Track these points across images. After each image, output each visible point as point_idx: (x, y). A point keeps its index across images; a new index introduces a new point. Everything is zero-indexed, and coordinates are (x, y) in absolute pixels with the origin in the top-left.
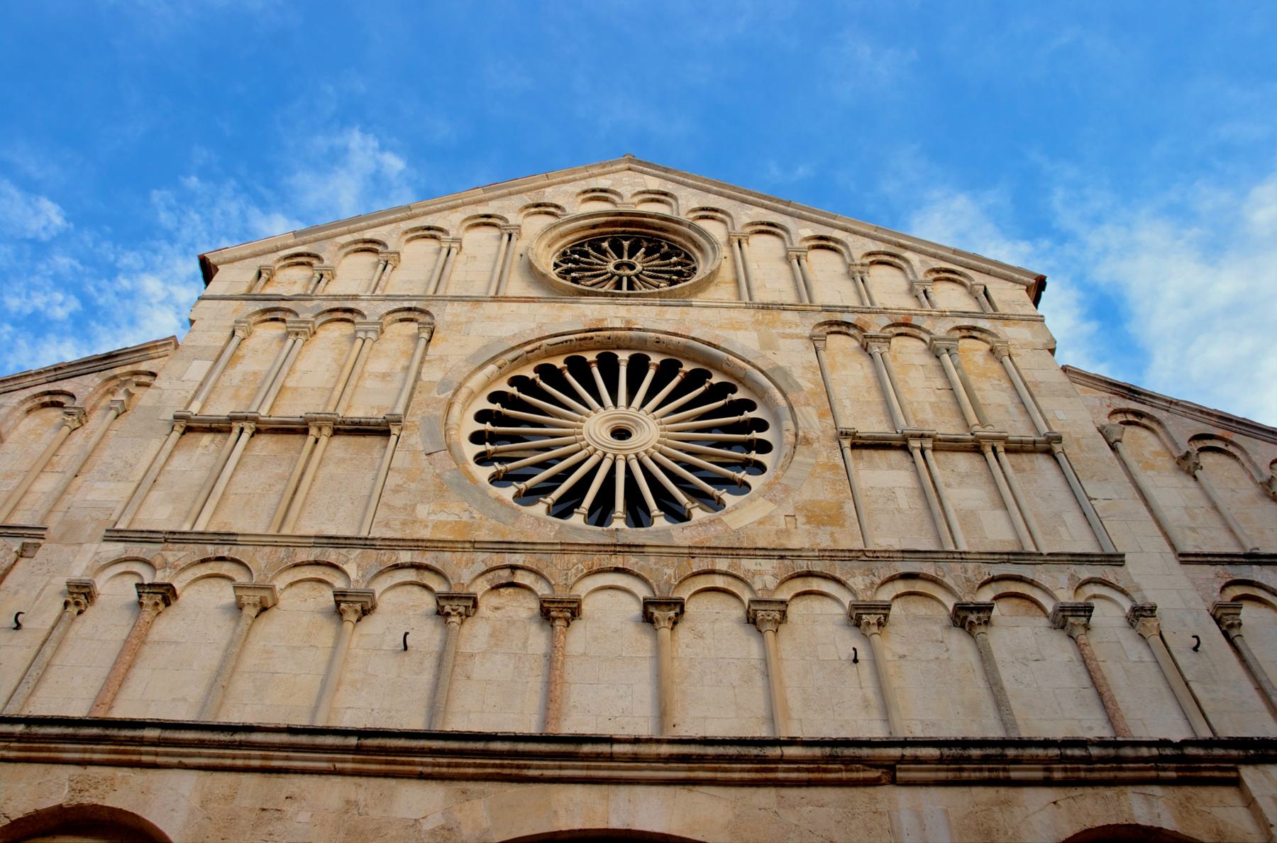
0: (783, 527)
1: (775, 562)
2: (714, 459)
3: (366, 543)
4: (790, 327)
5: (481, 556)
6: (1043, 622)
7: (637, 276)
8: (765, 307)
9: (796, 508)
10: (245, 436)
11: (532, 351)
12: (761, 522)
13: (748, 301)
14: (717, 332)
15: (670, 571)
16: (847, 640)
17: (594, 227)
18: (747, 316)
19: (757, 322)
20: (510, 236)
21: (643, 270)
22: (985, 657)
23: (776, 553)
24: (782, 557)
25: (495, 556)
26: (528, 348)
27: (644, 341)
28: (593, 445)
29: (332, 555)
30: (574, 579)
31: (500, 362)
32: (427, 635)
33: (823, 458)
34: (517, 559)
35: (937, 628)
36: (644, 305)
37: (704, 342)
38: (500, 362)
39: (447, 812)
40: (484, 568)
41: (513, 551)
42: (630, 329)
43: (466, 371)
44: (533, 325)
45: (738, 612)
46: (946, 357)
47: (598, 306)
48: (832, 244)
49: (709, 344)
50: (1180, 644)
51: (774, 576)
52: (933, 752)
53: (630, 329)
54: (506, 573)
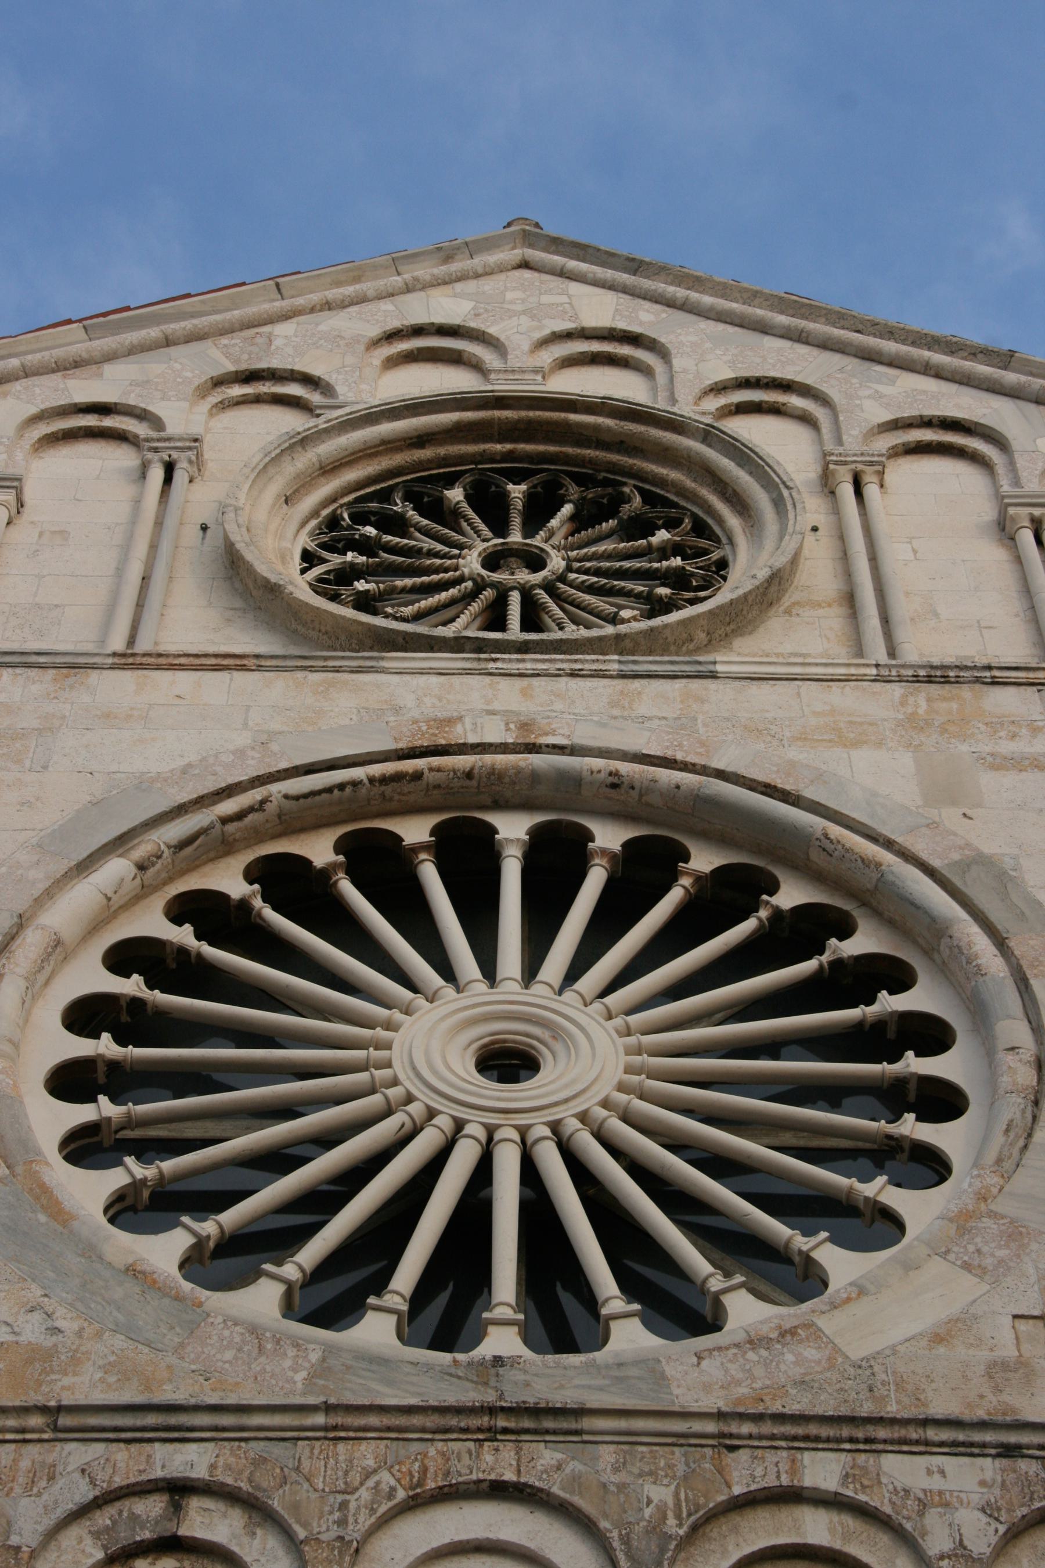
0: (1010, 1352)
1: (989, 1467)
2: (788, 1139)
4: (1013, 736)
7: (549, 587)
11: (240, 816)
12: (938, 1338)
13: (882, 657)
14: (793, 753)
15: (660, 1493)
17: (421, 440)
19: (914, 723)
20: (169, 468)
21: (569, 569)
23: (989, 1437)
24: (1009, 1451)
25: (121, 1454)
26: (229, 807)
27: (572, 781)
28: (426, 1098)
30: (365, 1521)
31: (142, 850)
36: (573, 674)
37: (752, 785)
38: (142, 850)
40: (84, 1493)
41: (181, 1435)
42: (533, 748)
43: (39, 878)
44: (242, 739)
47: (434, 680)
49: (769, 790)
51: (989, 1510)
53: (533, 748)
54: (152, 1507)
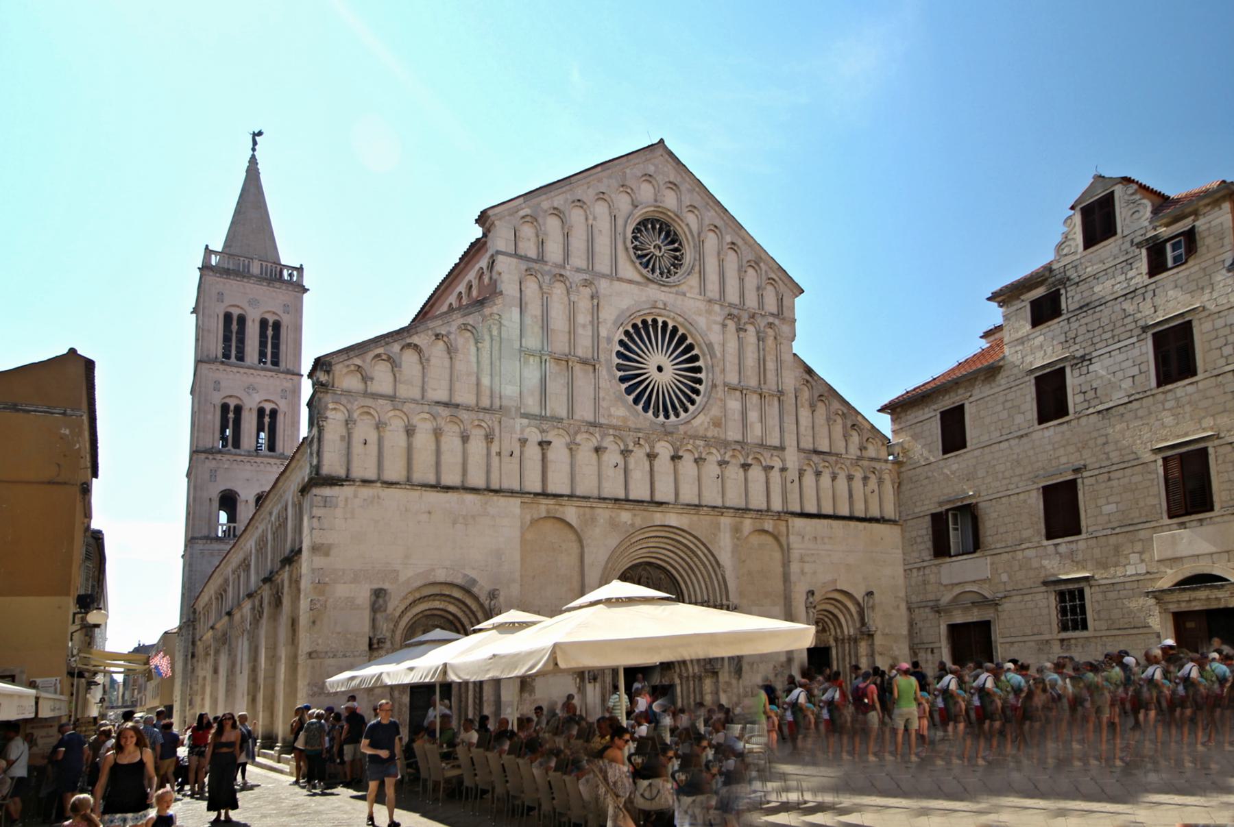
3: (601, 426)
5: (631, 433)
6: (760, 468)
8: (710, 301)
9: (711, 419)
10: (548, 363)
12: (702, 424)
16: (717, 470)
18: (702, 306)
22: (746, 479)
26: (632, 317)
29: (591, 429)
32: (619, 459)
33: (719, 396)
34: (640, 435)
35: (736, 468)
39: (632, 520)
45: (692, 458)
46: (761, 342)
48: (736, 248)
49: (690, 323)
50: (789, 480)
52: (732, 511)
53: (665, 309)
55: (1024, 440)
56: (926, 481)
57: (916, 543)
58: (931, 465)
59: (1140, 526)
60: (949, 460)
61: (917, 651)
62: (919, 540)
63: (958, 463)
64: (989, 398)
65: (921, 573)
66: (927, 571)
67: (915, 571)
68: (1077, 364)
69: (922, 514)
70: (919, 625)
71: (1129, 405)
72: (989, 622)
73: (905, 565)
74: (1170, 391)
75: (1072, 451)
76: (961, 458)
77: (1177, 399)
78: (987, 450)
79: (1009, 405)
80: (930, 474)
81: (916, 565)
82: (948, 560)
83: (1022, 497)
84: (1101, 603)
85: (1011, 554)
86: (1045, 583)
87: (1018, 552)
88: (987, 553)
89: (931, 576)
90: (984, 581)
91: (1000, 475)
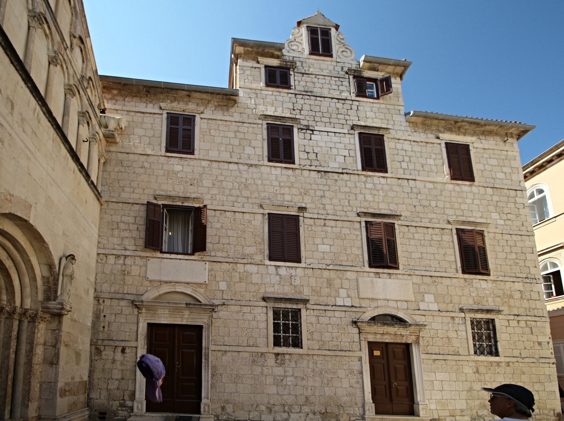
55: (252, 169)
56: (142, 171)
57: (118, 228)
58: (150, 157)
59: (348, 268)
60: (173, 159)
61: (102, 348)
62: (122, 226)
63: (183, 166)
64: (222, 122)
65: (121, 262)
66: (129, 261)
67: (111, 260)
68: (302, 129)
69: (131, 201)
70: (107, 318)
71: (341, 175)
72: (200, 328)
73: (98, 248)
74: (370, 176)
75: (295, 193)
76: (186, 163)
77: (374, 184)
78: (215, 165)
79: (240, 136)
80: (147, 165)
81: (115, 252)
82: (159, 255)
83: (247, 216)
84: (314, 325)
85: (231, 265)
86: (264, 299)
87: (238, 265)
88: (206, 258)
89: (133, 267)
90: (199, 285)
91: (227, 192)
